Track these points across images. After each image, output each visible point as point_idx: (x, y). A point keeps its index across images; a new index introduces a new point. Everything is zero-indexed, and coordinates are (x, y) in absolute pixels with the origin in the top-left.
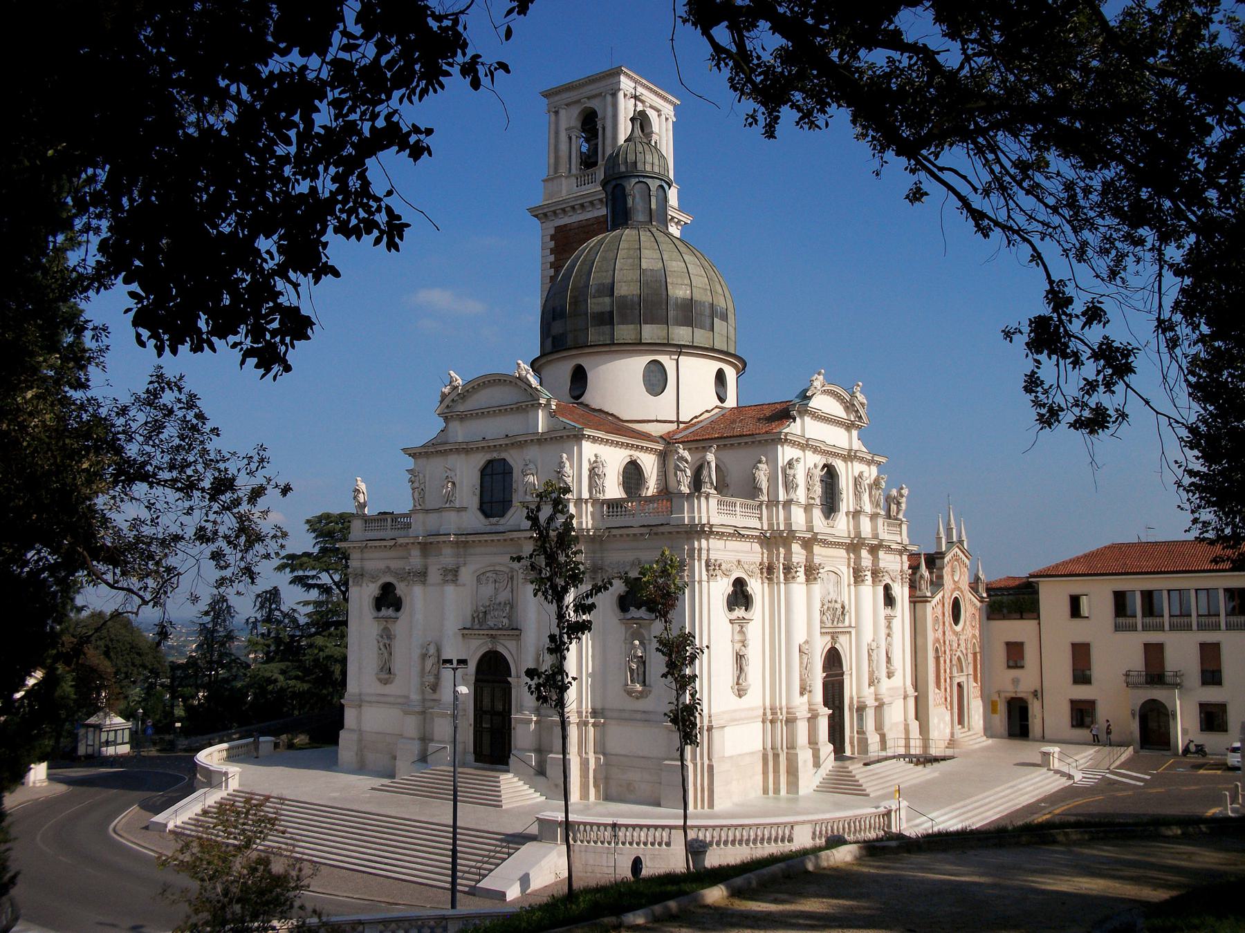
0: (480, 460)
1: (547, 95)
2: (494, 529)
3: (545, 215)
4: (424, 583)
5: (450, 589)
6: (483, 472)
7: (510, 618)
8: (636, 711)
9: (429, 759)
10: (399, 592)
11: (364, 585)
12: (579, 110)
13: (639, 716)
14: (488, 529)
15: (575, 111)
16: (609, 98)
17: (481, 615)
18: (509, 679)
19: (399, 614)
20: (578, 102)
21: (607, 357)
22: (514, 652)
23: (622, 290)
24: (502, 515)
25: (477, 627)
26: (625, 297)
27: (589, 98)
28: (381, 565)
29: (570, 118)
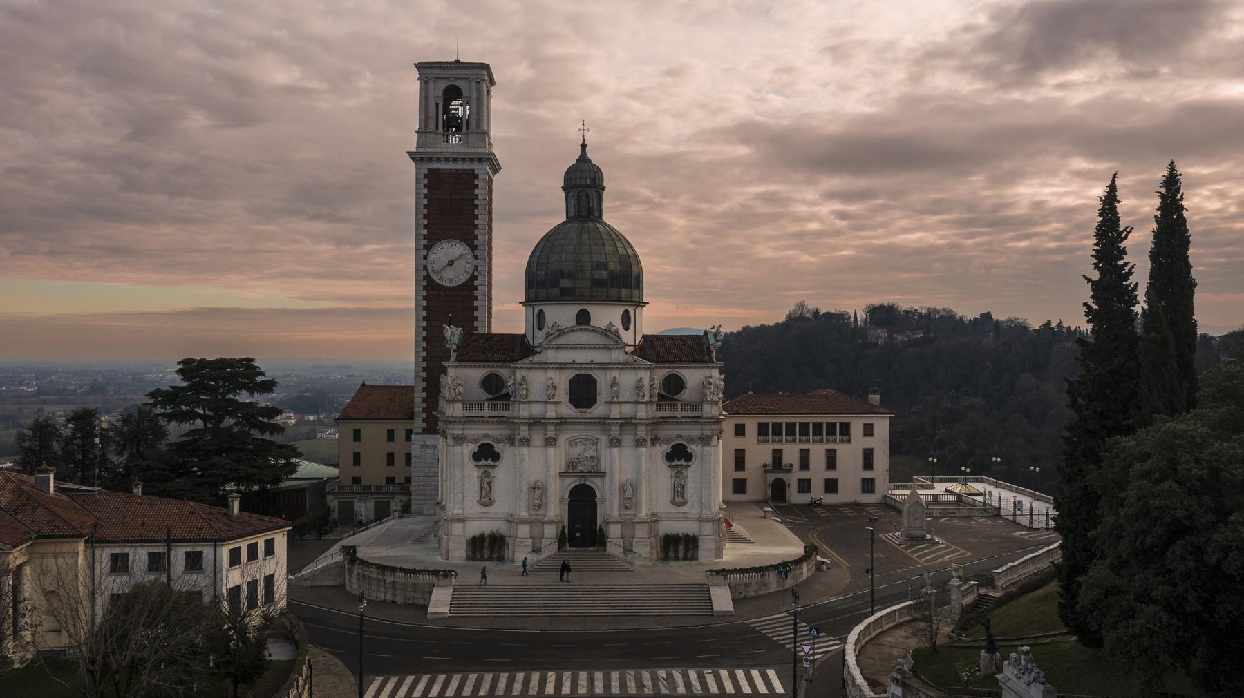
0: (569, 375)
1: (420, 66)
2: (583, 415)
3: (421, 159)
4: (528, 445)
5: (551, 450)
6: (571, 382)
7: (596, 465)
8: (679, 513)
9: (543, 550)
10: (496, 450)
11: (465, 445)
12: (444, 86)
13: (680, 516)
14: (578, 415)
15: (443, 85)
16: (474, 84)
17: (574, 464)
18: (596, 500)
19: (496, 464)
20: (448, 79)
21: (614, 306)
22: (599, 484)
23: (612, 267)
24: (589, 406)
25: (571, 471)
26: (613, 271)
27: (456, 79)
28: (481, 433)
29: (438, 90)
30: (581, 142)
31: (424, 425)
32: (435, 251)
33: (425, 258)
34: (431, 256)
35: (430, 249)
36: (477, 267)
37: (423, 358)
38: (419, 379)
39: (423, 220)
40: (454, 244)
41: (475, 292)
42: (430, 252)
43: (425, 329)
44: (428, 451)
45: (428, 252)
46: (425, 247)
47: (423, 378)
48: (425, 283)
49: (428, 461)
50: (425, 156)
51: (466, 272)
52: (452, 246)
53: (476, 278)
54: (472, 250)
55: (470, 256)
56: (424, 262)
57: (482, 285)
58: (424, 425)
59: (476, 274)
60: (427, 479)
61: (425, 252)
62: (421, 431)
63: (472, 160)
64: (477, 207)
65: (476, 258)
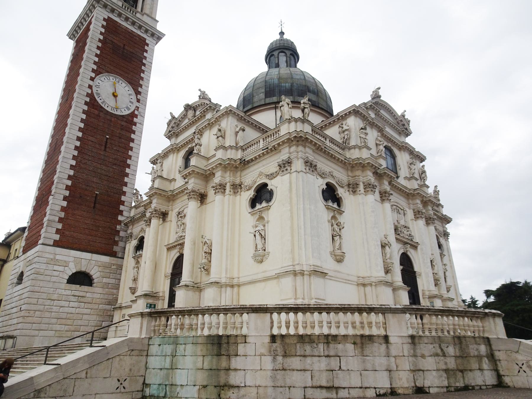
30: (280, 31)
31: (57, 237)
32: (102, 79)
33: (92, 79)
34: (97, 80)
35: (98, 75)
36: (138, 108)
37: (71, 166)
38: (62, 185)
39: (96, 50)
40: (121, 82)
41: (134, 127)
42: (97, 77)
43: (78, 139)
44: (56, 268)
45: (96, 76)
46: (93, 71)
47: (67, 186)
48: (88, 100)
49: (54, 279)
50: (111, 5)
51: (128, 109)
52: (118, 82)
53: (136, 116)
54: (136, 93)
55: (134, 97)
56: (91, 83)
57: (140, 124)
58: (57, 237)
59: (136, 112)
60: (48, 302)
61: (93, 75)
62: (52, 243)
63: (146, 31)
64: (144, 65)
65: (138, 101)
